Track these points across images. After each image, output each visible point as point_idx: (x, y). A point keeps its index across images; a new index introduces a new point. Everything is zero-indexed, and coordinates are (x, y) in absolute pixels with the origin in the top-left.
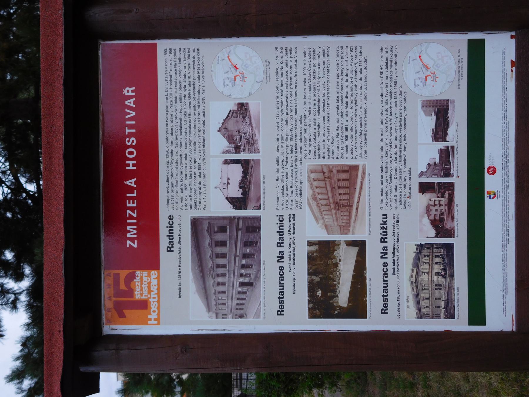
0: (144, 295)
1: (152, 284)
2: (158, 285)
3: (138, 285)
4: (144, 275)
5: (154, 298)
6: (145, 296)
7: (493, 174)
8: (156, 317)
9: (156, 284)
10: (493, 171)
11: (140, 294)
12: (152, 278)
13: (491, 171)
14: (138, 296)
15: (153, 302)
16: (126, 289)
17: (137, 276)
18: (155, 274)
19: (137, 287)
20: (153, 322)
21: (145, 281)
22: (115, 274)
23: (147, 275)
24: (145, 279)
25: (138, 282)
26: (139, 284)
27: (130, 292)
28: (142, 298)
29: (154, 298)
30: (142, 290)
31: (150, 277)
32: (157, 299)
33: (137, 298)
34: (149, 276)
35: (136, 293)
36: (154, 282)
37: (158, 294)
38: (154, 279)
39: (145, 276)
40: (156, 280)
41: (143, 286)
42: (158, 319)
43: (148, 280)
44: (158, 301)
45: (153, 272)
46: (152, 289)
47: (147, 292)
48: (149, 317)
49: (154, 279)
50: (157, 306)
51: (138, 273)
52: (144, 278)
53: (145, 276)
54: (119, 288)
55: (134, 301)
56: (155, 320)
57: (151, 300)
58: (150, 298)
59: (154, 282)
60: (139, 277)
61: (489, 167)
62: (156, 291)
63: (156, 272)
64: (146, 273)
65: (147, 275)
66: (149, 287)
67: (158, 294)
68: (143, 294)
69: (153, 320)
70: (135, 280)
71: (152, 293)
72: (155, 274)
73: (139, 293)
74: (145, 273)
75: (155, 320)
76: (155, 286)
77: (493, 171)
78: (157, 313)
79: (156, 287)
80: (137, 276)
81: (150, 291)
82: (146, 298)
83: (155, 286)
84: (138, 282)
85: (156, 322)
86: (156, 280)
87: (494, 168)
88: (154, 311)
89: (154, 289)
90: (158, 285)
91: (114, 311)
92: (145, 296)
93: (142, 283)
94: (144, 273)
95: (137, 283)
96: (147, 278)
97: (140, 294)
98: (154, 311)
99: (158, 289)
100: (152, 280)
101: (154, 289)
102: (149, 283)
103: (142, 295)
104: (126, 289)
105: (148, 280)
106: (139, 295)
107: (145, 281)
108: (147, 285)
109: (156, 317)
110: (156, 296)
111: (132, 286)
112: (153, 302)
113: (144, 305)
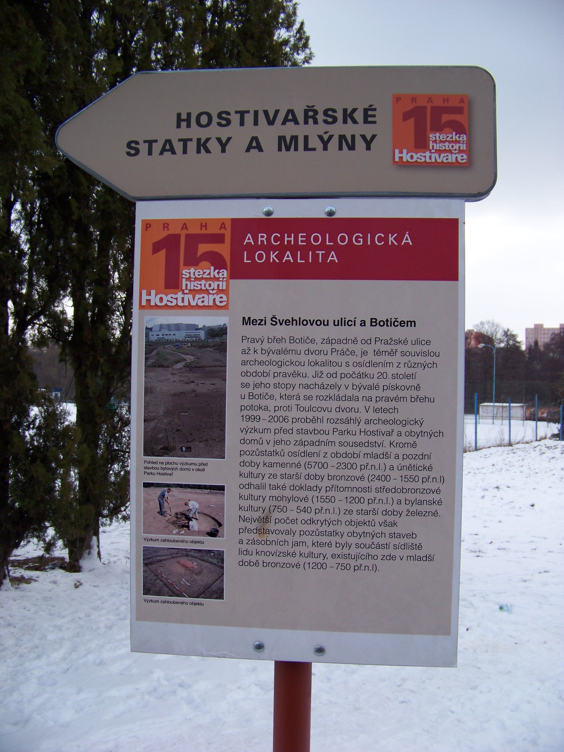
0: (188, 283)
4: (220, 283)
5: (183, 298)
6: (186, 285)
8: (153, 304)
9: (206, 304)
11: (190, 277)
14: (185, 272)
16: (199, 254)
17: (218, 273)
18: (221, 302)
19: (201, 273)
20: (145, 297)
21: (210, 285)
22: (223, 235)
23: (221, 288)
25: (209, 274)
26: (205, 276)
27: (193, 261)
28: (184, 280)
29: (183, 298)
30: (196, 279)
31: (217, 294)
32: (182, 304)
33: (184, 272)
35: (192, 270)
37: (190, 307)
38: (214, 299)
39: (218, 285)
40: (211, 304)
42: (149, 306)
43: (213, 290)
46: (198, 296)
47: (192, 288)
48: (153, 292)
49: (214, 299)
50: (169, 304)
52: (216, 283)
53: (218, 285)
54: (201, 243)
55: (179, 269)
56: (149, 301)
57: (180, 295)
58: (183, 293)
60: (217, 276)
62: (193, 303)
65: (221, 288)
66: (201, 291)
67: (190, 307)
68: (190, 281)
70: (212, 268)
71: (190, 296)
72: (221, 302)
73: (192, 276)
75: (149, 301)
76: (203, 302)
78: (159, 304)
79: (200, 304)
80: (218, 273)
81: (193, 292)
82: (184, 288)
83: (203, 302)
84: (209, 274)
85: (144, 303)
86: (211, 304)
88: (161, 300)
89: (197, 300)
91: (164, 234)
92: (186, 285)
95: (208, 271)
96: (216, 288)
97: (190, 277)
98: (161, 300)
99: (197, 307)
100: (211, 297)
101: (197, 300)
102: (207, 292)
103: (189, 279)
104: (199, 254)
106: (188, 276)
107: (210, 285)
108: (203, 288)
109: (153, 304)
110: (186, 303)
113: (172, 283)
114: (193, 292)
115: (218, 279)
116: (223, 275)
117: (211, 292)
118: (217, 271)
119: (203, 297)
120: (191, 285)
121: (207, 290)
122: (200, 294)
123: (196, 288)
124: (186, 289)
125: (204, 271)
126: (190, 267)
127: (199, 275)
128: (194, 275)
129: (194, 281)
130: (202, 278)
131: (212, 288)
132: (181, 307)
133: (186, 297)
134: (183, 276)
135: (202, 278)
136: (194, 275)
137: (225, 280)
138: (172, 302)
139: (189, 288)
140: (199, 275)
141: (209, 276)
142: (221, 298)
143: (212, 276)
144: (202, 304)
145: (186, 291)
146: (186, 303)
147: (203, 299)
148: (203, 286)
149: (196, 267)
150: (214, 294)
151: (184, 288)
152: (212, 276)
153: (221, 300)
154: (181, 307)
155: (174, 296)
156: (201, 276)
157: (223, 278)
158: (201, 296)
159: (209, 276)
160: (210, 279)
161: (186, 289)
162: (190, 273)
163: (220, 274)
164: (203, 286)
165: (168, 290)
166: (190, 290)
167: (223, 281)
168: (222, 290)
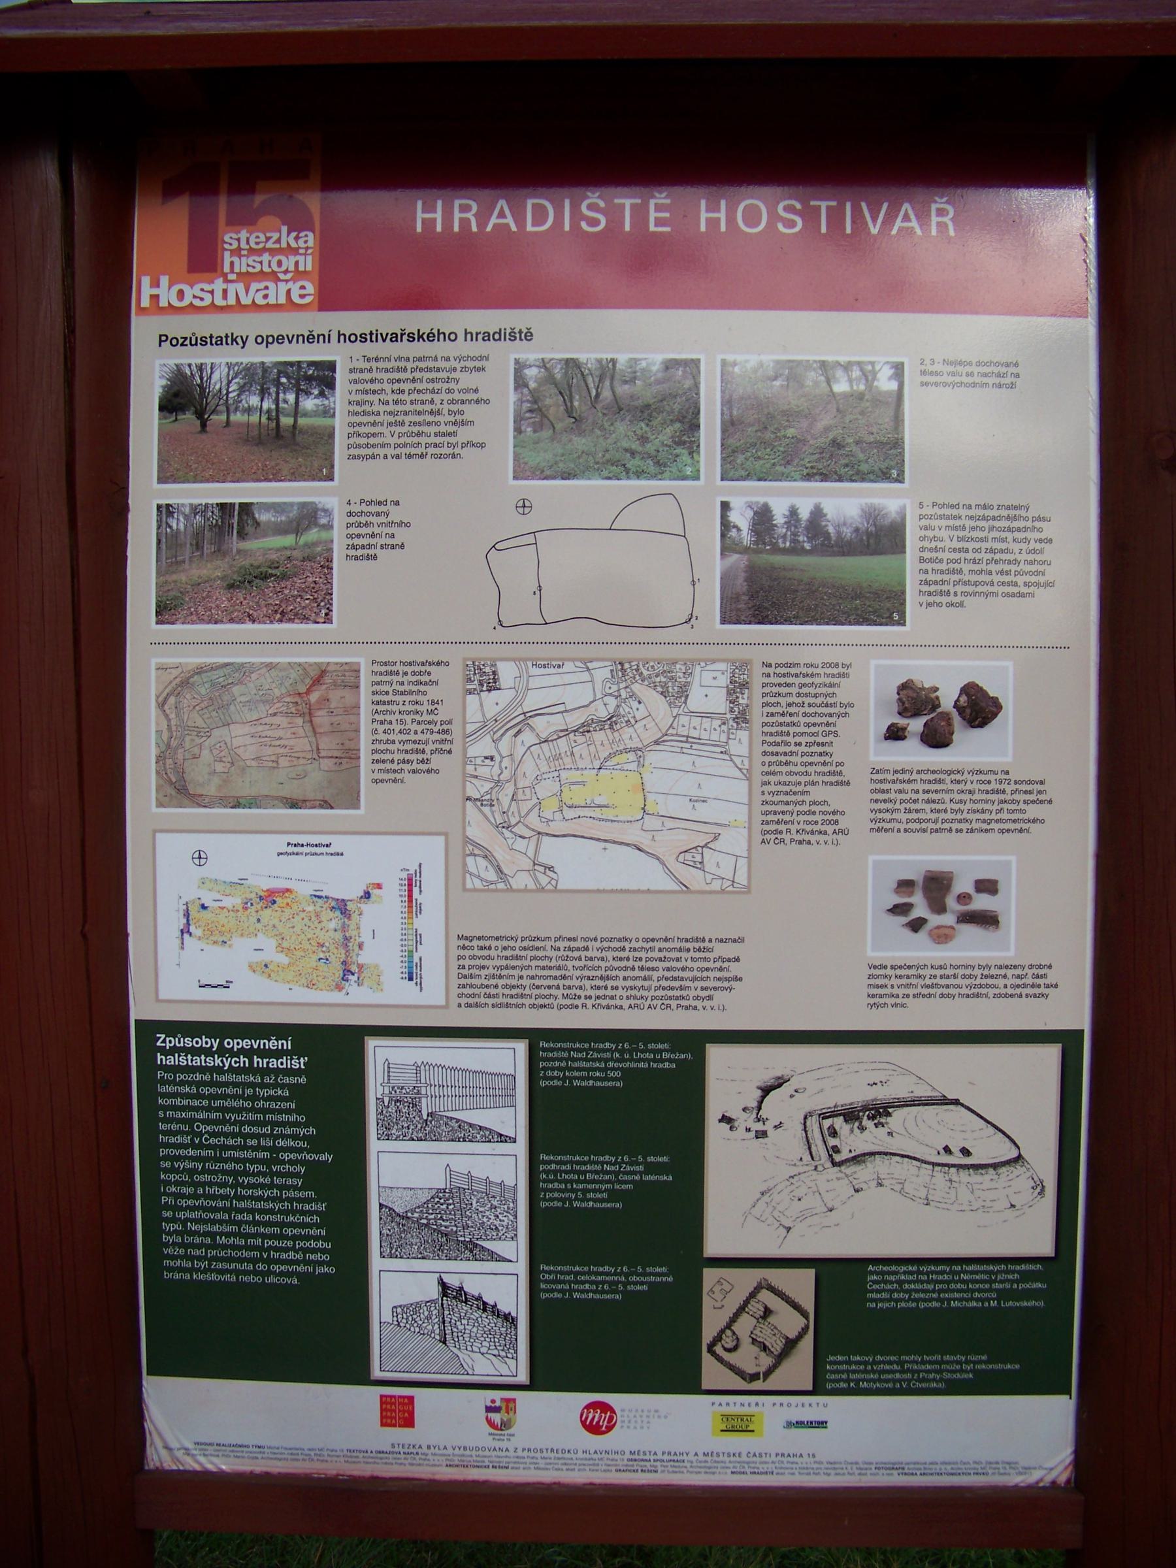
0: (236, 260)
1: (271, 285)
2: (269, 307)
3: (268, 239)
4: (301, 259)
5: (225, 292)
6: (232, 264)
7: (583, 1423)
10: (598, 1422)
11: (239, 249)
12: (290, 285)
13: (596, 1416)
14: (229, 239)
15: (212, 292)
17: (297, 238)
18: (302, 296)
19: (263, 238)
21: (280, 264)
24: (289, 263)
25: (278, 241)
26: (270, 245)
28: (227, 254)
29: (225, 292)
30: (252, 251)
33: (227, 238)
34: (299, 275)
35: (244, 235)
36: (277, 293)
38: (289, 291)
39: (297, 263)
40: (282, 300)
41: (266, 257)
43: (286, 272)
44: (213, 308)
45: (310, 289)
46: (254, 286)
47: (244, 270)
49: (289, 291)
51: (310, 239)
52: (293, 259)
53: (297, 263)
58: (227, 281)
59: (277, 293)
60: (293, 245)
61: (613, 1411)
62: (246, 301)
63: (308, 300)
64: (309, 268)
65: (301, 268)
68: (240, 256)
69: (155, 291)
70: (284, 229)
71: (240, 287)
72: (302, 296)
73: (243, 245)
74: (307, 263)
76: (266, 297)
77: (598, 1422)
79: (260, 301)
80: (297, 238)
82: (227, 269)
83: (266, 297)
86: (282, 300)
87: (610, 1428)
88: (181, 294)
89: (254, 294)
90: (269, 307)
92: (232, 264)
93: (273, 252)
94: (309, 258)
95: (275, 236)
96: (292, 268)
97: (239, 249)
101: (254, 294)
102: (274, 277)
103: (237, 252)
105: (286, 272)
106: (235, 245)
107: (280, 264)
108: (266, 269)
110: (232, 301)
111: (264, 221)
112: (212, 292)
113: (203, 260)
114: (247, 278)
115: (295, 251)
116: (306, 242)
117: (281, 276)
118: (294, 234)
119: (266, 288)
120: (242, 265)
121: (274, 273)
122: (260, 282)
123: (251, 270)
124: (232, 271)
125: (268, 235)
126: (238, 228)
127: (257, 243)
128: (248, 242)
129: (248, 256)
130: (265, 250)
131: (284, 268)
132: (222, 309)
133: (232, 288)
134: (226, 246)
135: (265, 250)
136: (248, 242)
137: (310, 251)
138: (202, 299)
139: (237, 270)
140: (257, 243)
141: (277, 246)
142: (303, 287)
143: (284, 245)
144: (264, 302)
145: (232, 277)
146: (232, 301)
147: (266, 292)
148: (265, 264)
149: (251, 228)
150: (287, 281)
151: (227, 269)
152: (284, 245)
153: (303, 292)
154: (222, 309)
155: (207, 287)
156: (261, 246)
157: (307, 248)
158: (262, 285)
159: (277, 246)
160: (280, 251)
161: (232, 271)
162: (238, 240)
163: (301, 243)
164: (265, 264)
165: (197, 276)
166: (239, 274)
167: (305, 254)
168: (305, 272)
